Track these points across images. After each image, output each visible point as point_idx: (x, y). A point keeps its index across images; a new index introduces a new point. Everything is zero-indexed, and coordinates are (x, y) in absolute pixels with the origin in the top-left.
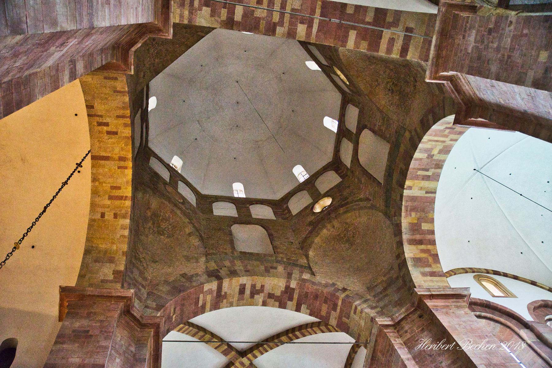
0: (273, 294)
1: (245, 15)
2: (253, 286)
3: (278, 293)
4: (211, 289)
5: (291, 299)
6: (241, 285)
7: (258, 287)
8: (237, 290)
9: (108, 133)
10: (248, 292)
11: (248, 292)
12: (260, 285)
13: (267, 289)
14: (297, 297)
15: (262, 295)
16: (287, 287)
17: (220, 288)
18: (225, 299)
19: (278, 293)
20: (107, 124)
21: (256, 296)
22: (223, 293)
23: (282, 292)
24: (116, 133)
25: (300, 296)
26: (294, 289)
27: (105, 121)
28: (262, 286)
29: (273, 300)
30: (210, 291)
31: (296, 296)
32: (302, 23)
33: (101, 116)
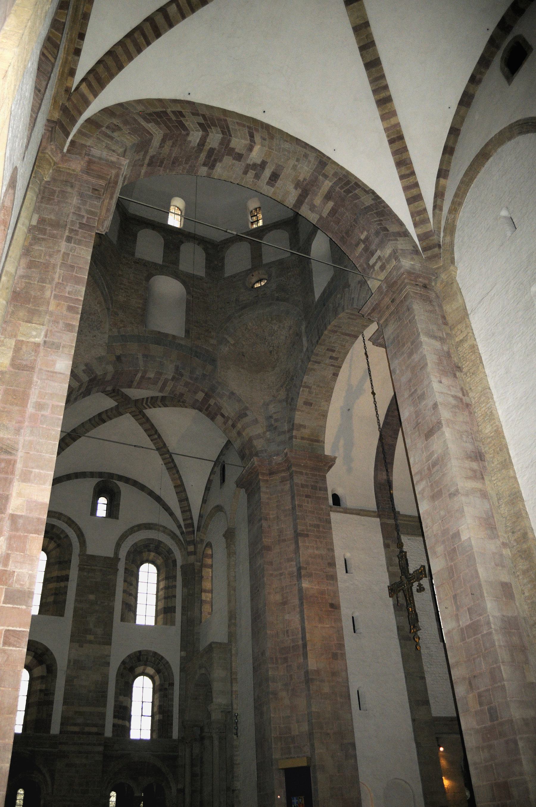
0: (234, 159)
1: (195, 393)
2: (257, 177)
3: (228, 160)
4: (310, 209)
5: (211, 151)
6: (273, 186)
7: (251, 174)
8: (279, 183)
9: (333, 351)
10: (267, 173)
11: (267, 173)
12: (248, 175)
13: (239, 166)
14: (202, 155)
15: (249, 162)
16: (212, 167)
17: (300, 201)
18: (299, 181)
19: (228, 160)
20: (331, 358)
21: (259, 162)
22: (299, 191)
23: (221, 161)
24: (328, 350)
25: (197, 158)
26: (204, 165)
27: (331, 361)
28: (245, 173)
29: (236, 150)
30: (312, 208)
31: (203, 156)
32: (150, 378)
33: (332, 365)
